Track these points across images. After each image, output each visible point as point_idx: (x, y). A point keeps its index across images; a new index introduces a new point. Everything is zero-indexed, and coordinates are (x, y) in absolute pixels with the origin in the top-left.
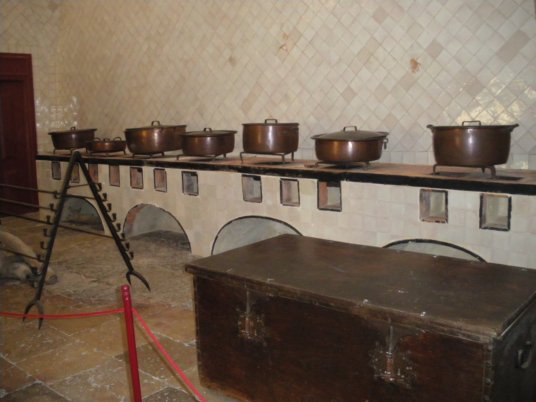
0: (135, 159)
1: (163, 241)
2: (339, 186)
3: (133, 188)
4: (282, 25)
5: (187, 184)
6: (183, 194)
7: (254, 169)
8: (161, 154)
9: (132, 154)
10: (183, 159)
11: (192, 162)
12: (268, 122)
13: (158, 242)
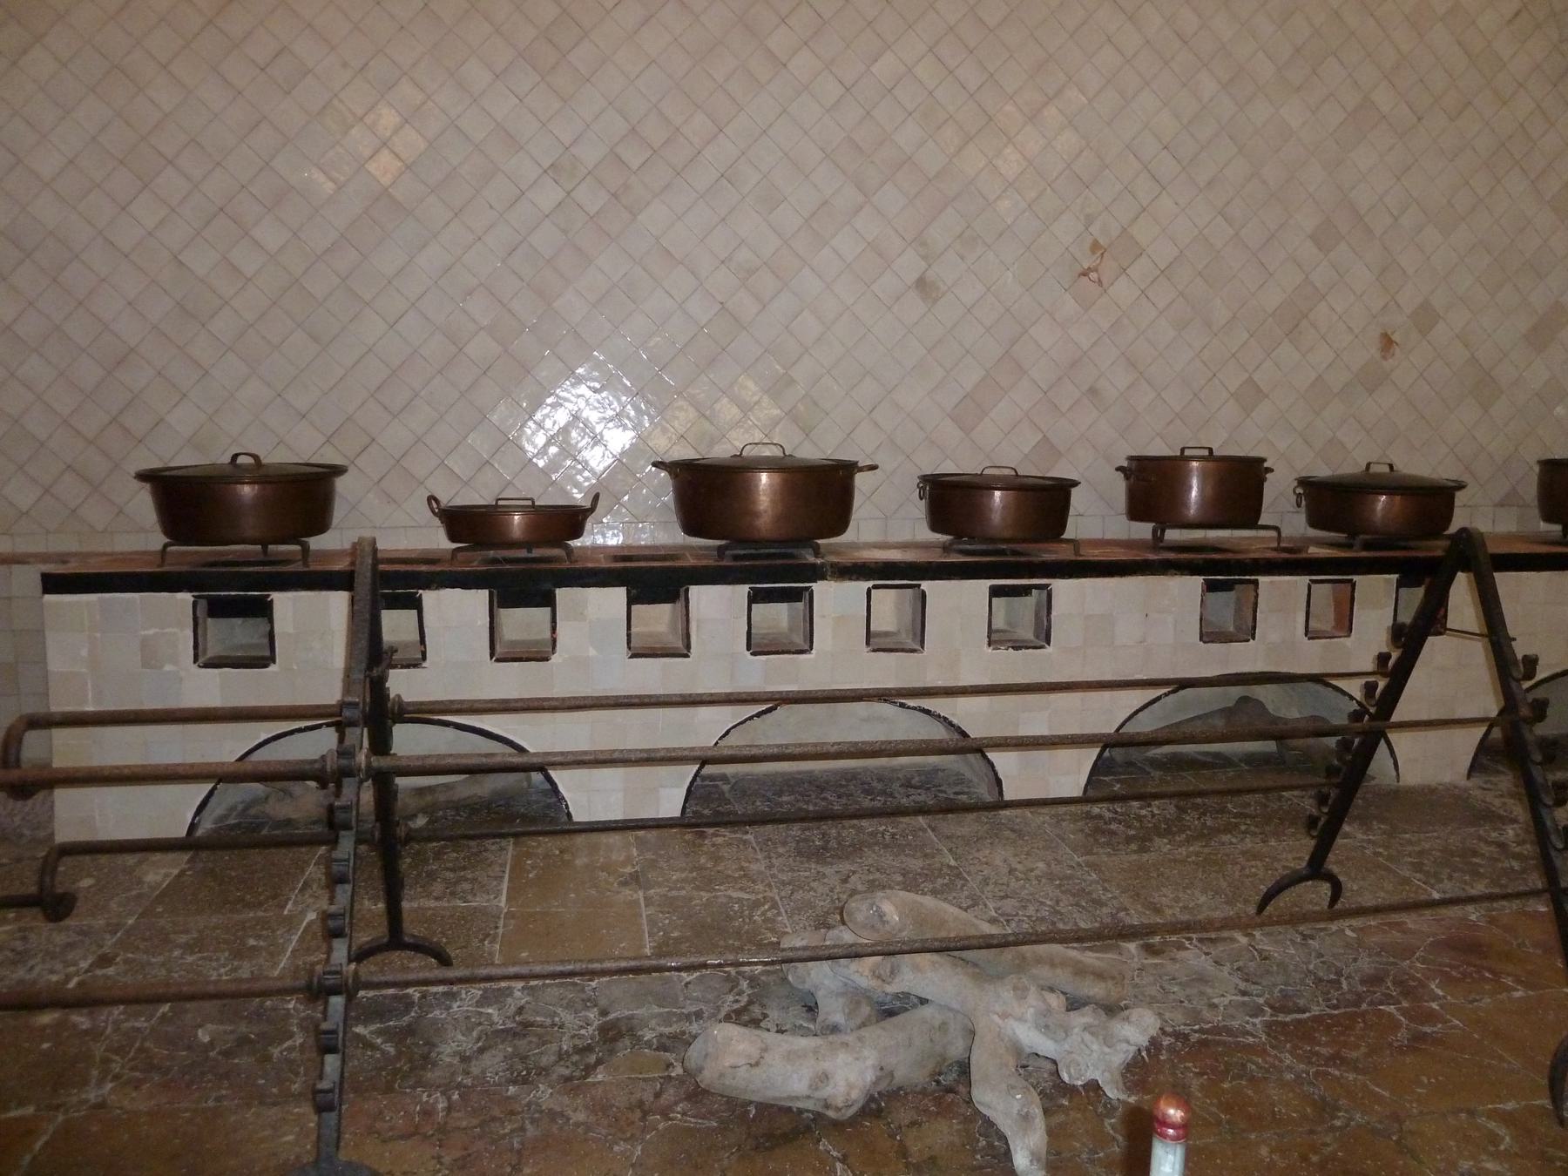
2: (549, 601)
4: (1089, 220)
12: (1187, 453)
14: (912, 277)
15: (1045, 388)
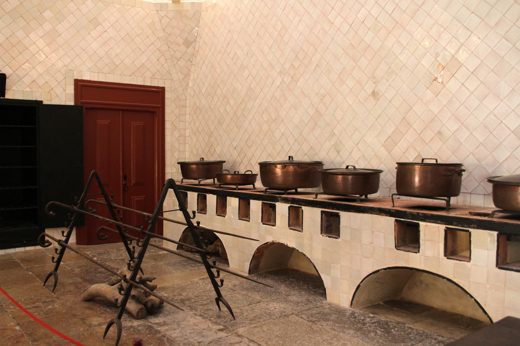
0: (267, 194)
1: (292, 281)
3: (263, 224)
5: (326, 225)
6: (321, 236)
7: (411, 213)
8: (294, 191)
9: (264, 188)
10: (322, 197)
11: (329, 201)
13: (287, 282)
14: (370, 92)
15: (419, 132)
